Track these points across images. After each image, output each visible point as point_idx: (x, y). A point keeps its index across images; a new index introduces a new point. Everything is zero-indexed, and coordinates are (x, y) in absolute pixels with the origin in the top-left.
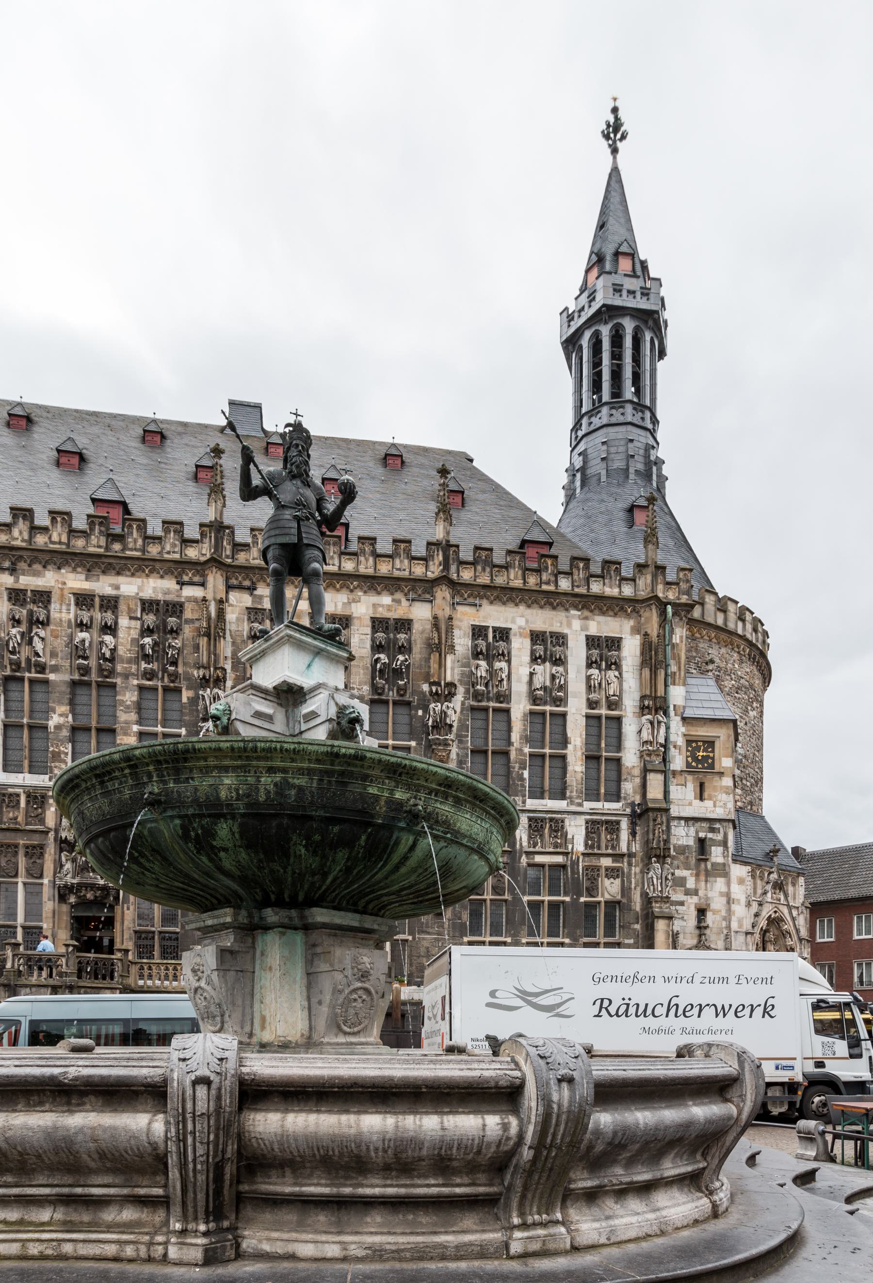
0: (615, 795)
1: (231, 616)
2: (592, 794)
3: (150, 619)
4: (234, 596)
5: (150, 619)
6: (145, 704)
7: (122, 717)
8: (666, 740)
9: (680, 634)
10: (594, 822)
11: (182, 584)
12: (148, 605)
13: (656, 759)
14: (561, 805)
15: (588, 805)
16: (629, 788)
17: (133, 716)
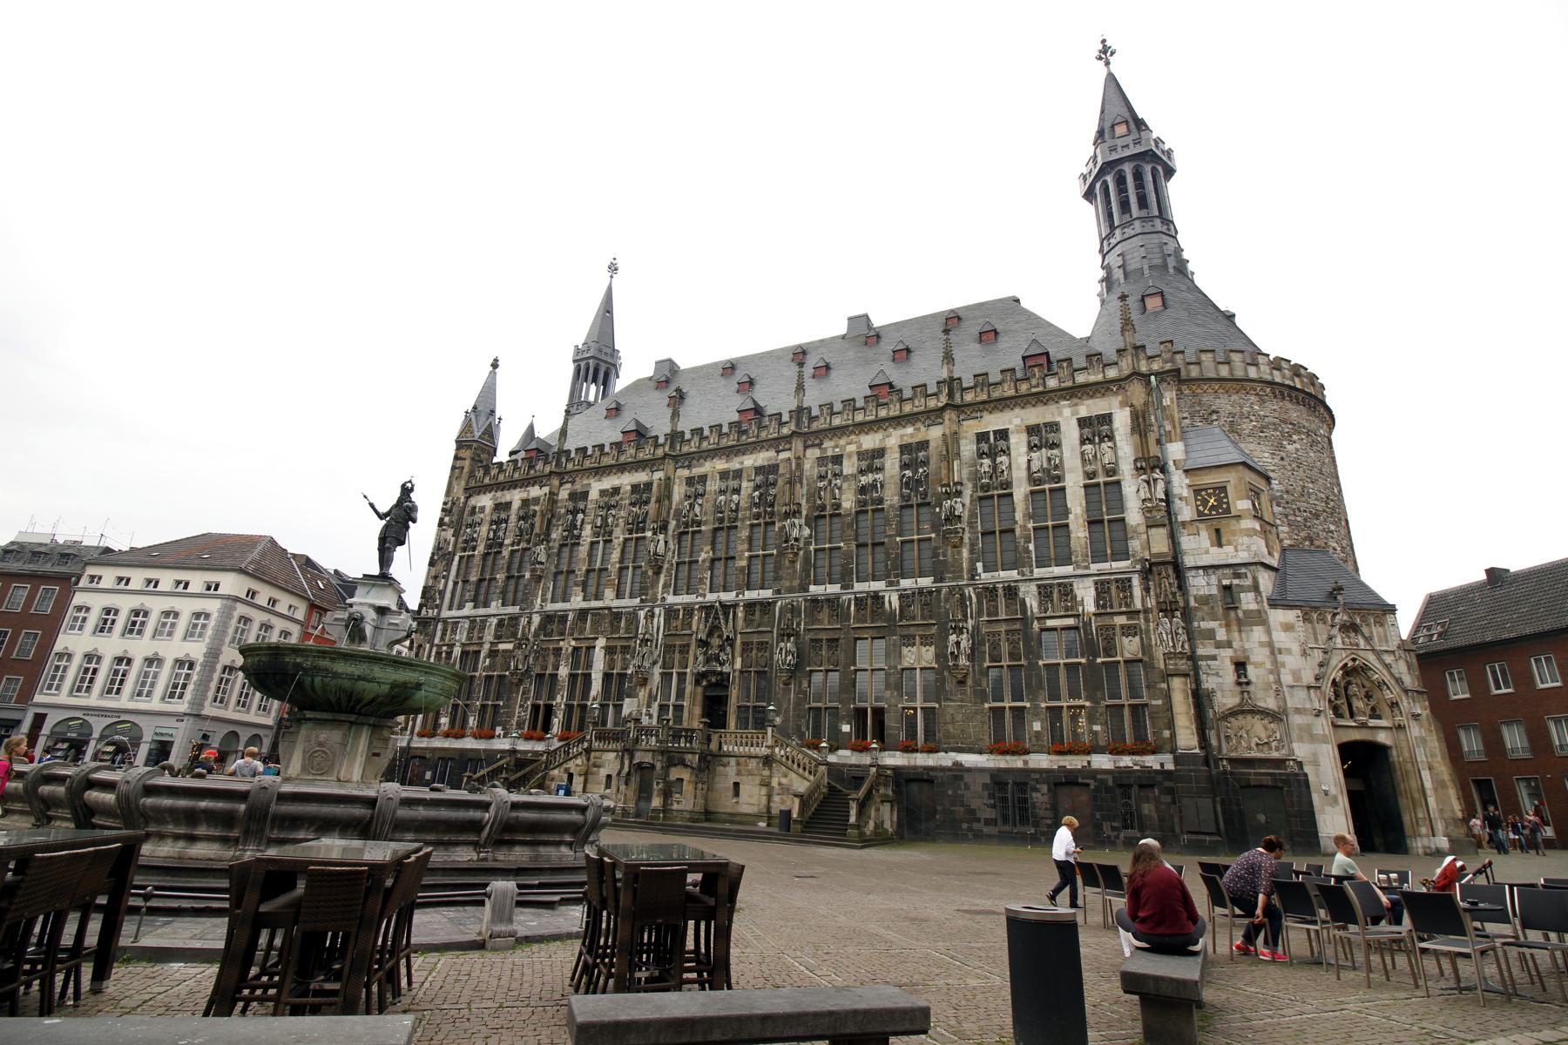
0: (1124, 554)
1: (807, 466)
2: (1098, 556)
3: (759, 479)
4: (809, 452)
5: (759, 479)
6: (756, 536)
7: (740, 548)
8: (1167, 495)
9: (1169, 397)
10: (1102, 582)
11: (778, 452)
12: (759, 470)
13: (1163, 514)
14: (1068, 570)
15: (1094, 568)
16: (1135, 545)
17: (746, 546)
